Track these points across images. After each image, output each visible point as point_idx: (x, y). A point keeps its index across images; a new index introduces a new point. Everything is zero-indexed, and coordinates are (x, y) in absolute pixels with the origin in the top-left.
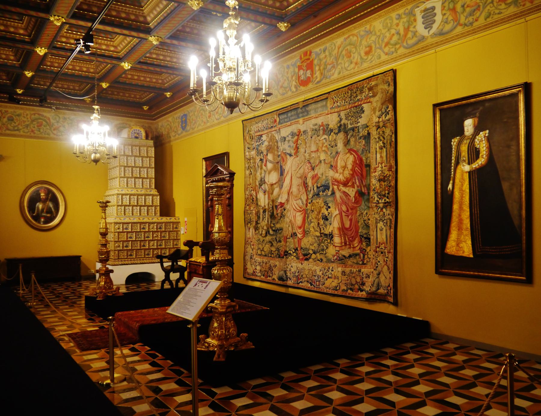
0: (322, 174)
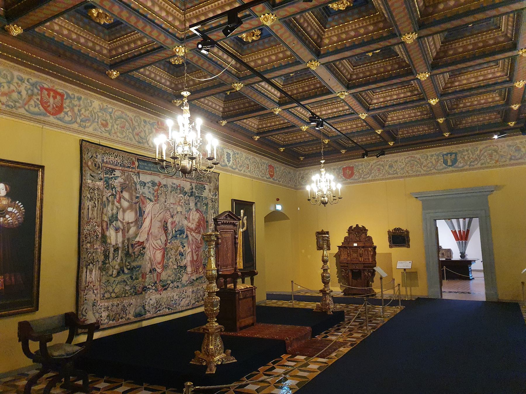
0: (179, 222)
